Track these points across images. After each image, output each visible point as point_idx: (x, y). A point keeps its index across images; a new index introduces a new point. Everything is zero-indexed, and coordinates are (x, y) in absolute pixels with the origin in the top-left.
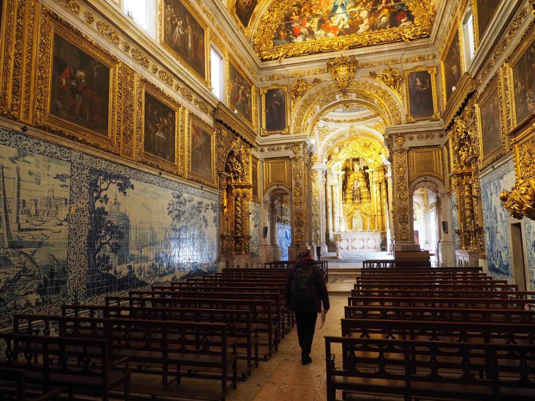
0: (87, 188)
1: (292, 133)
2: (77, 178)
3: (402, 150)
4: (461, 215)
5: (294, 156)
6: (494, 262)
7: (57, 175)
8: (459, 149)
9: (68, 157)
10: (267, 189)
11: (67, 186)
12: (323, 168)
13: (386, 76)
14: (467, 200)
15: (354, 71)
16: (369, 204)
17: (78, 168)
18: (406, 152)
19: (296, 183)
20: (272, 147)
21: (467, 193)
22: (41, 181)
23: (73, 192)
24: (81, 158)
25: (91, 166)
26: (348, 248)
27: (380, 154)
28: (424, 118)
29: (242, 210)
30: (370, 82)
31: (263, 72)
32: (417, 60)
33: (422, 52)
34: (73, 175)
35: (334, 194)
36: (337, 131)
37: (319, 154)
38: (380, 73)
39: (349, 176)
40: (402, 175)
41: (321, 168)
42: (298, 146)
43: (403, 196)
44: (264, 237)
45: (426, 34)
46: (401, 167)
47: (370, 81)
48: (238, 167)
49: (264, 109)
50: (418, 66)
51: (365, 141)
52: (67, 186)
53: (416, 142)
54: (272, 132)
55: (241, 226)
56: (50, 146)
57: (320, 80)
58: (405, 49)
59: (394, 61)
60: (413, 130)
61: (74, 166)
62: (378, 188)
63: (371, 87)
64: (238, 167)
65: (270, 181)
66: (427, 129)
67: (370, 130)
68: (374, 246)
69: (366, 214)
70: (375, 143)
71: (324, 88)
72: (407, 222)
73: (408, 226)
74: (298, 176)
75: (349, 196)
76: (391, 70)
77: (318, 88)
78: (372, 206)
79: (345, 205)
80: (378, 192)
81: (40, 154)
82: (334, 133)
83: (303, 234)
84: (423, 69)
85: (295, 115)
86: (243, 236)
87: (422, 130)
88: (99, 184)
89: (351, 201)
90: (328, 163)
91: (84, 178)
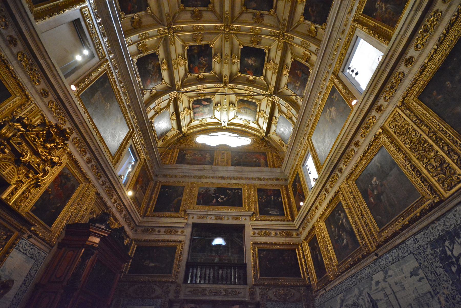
0: (441, 267)
2: (426, 263)
7: (411, 273)
9: (407, 251)
11: (423, 278)
17: (420, 253)
22: (405, 286)
23: (431, 280)
24: (416, 241)
25: (429, 240)
34: (421, 263)
52: (423, 278)
56: (393, 253)
61: (416, 254)
81: (392, 264)
88: (449, 253)
91: (431, 259)
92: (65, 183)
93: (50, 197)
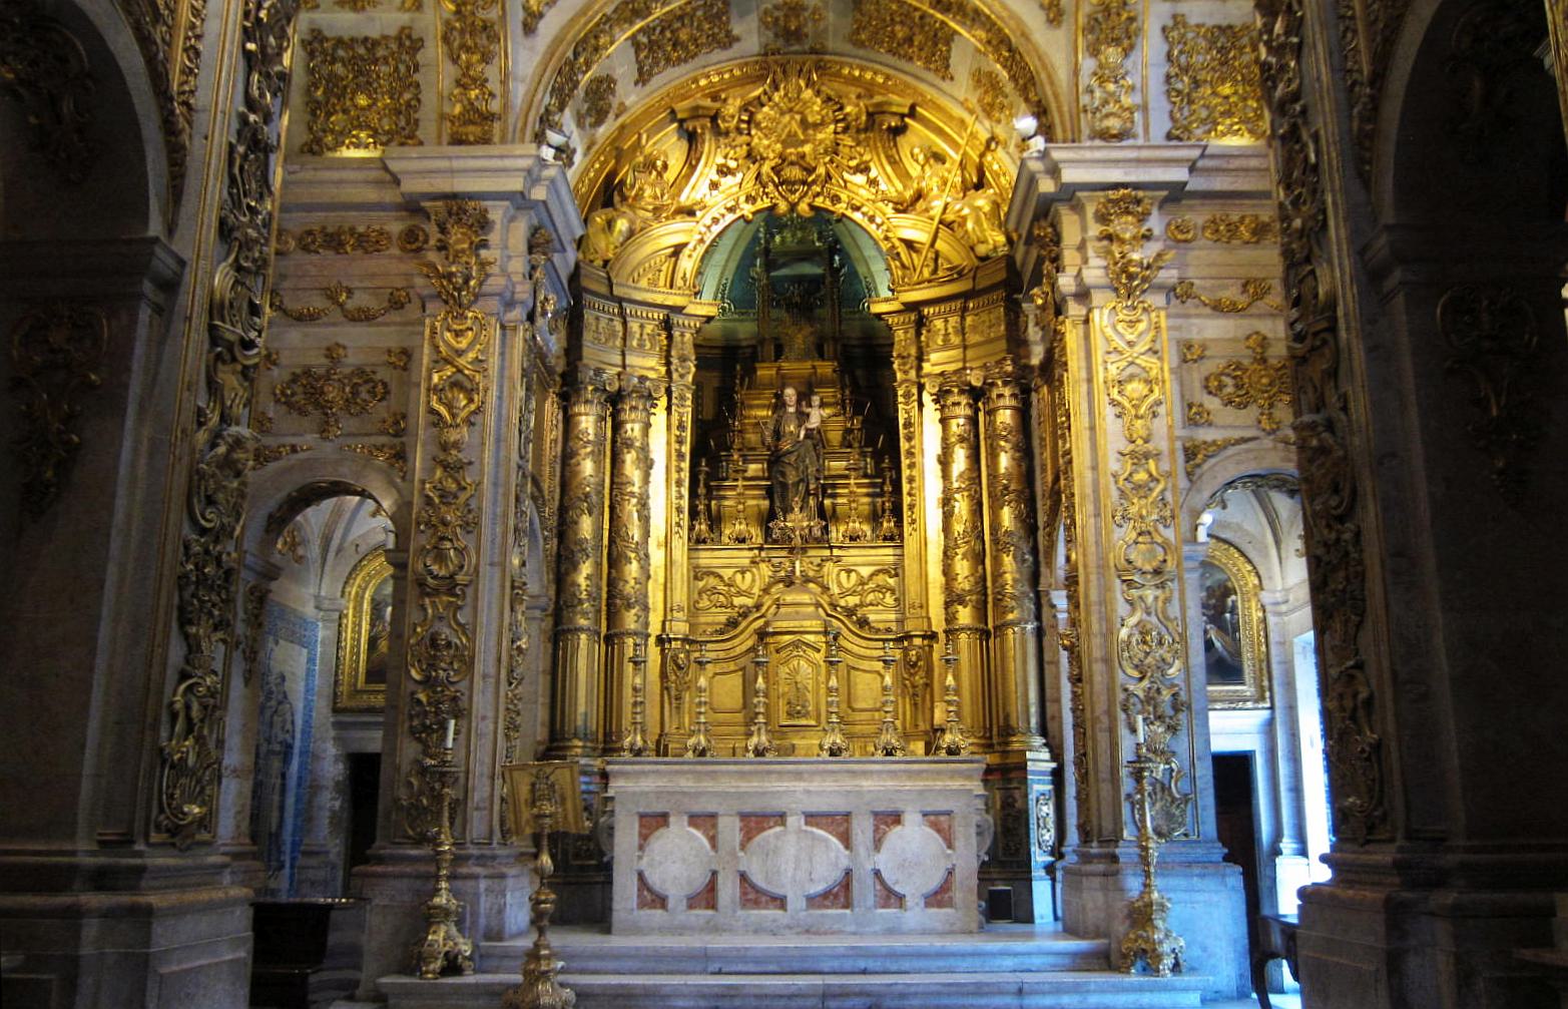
12: (539, 193)
16: (886, 555)
26: (708, 897)
27: (980, 185)
35: (630, 458)
37: (519, 92)
39: (750, 371)
41: (516, 184)
51: (869, 89)
62: (958, 426)
68: (934, 882)
69: (863, 623)
75: (742, 498)
78: (911, 566)
79: (707, 558)
89: (756, 534)
90: (599, 219)
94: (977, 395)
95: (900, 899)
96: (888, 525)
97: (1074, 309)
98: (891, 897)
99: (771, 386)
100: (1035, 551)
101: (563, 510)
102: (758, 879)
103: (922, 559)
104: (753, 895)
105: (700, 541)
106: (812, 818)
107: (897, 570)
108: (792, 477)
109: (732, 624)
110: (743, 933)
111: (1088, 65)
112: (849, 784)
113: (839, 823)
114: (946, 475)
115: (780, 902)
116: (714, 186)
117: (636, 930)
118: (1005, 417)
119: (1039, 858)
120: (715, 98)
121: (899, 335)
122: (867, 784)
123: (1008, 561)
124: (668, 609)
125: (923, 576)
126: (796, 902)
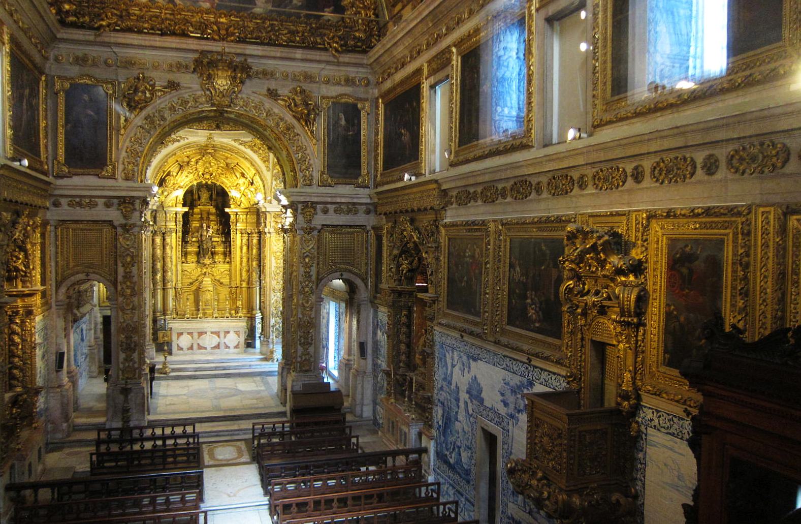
1: (119, 178)
3: (311, 229)
4: (393, 349)
5: (124, 222)
6: (448, 453)
8: (400, 256)
10: (64, 279)
13: (294, 99)
14: (404, 329)
15: (242, 82)
16: (227, 266)
18: (315, 233)
19: (126, 273)
20: (78, 200)
21: (404, 319)
26: (191, 348)
28: (348, 181)
29: (23, 340)
30: (267, 106)
31: (62, 46)
32: (343, 83)
33: (352, 72)
35: (168, 248)
36: (182, 142)
38: (284, 91)
40: (308, 270)
42: (133, 204)
43: (307, 302)
44: (57, 371)
45: (361, 47)
46: (307, 256)
47: (268, 104)
48: (19, 258)
49: (61, 122)
50: (345, 95)
51: (227, 158)
53: (333, 219)
54: (80, 171)
55: (22, 370)
57: (178, 85)
58: (328, 62)
59: (308, 77)
60: (329, 200)
62: (245, 241)
63: (269, 114)
64: (19, 258)
65: (71, 265)
66: (351, 201)
67: (242, 148)
69: (221, 283)
70: (245, 165)
71: (187, 102)
72: (311, 344)
73: (311, 350)
74: (129, 259)
76: (303, 92)
77: (175, 99)
78: (233, 271)
79: (185, 266)
80: (245, 248)
82: (177, 144)
83: (136, 365)
84: (351, 101)
85: (127, 143)
86: (27, 390)
87: (343, 200)
92: (691, 271)
93: (679, 321)
94: (249, 234)
95: (229, 347)
96: (228, 259)
97: (268, 235)
98: (227, 347)
99: (198, 214)
100: (260, 271)
101: (153, 263)
102: (201, 344)
103: (236, 271)
104: (200, 347)
105: (183, 263)
106: (212, 333)
107: (230, 270)
108: (205, 247)
109: (191, 284)
110: (199, 356)
111: (274, 183)
112: (219, 324)
113: (217, 334)
114: (241, 252)
115: (206, 348)
116: (187, 176)
117: (177, 355)
118: (255, 241)
119: (258, 335)
120: (188, 157)
121: (232, 216)
122: (223, 324)
123: (254, 274)
124: (176, 281)
125: (236, 273)
126: (209, 349)
